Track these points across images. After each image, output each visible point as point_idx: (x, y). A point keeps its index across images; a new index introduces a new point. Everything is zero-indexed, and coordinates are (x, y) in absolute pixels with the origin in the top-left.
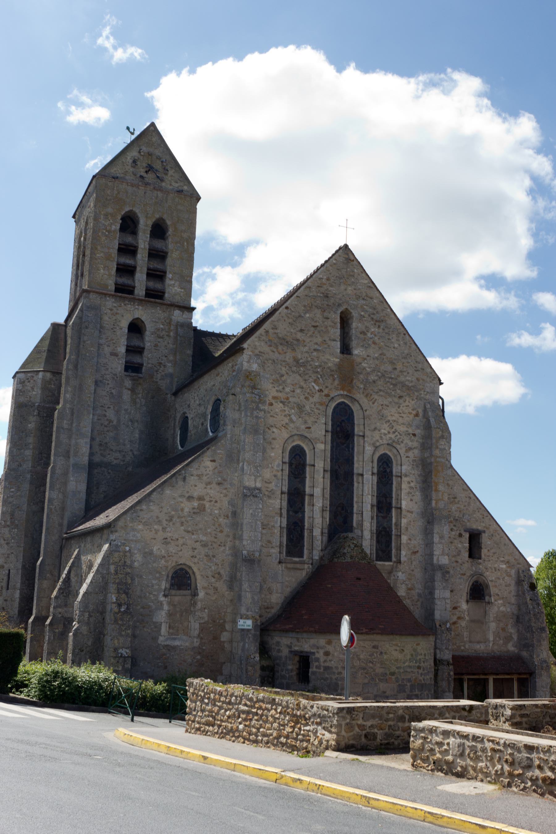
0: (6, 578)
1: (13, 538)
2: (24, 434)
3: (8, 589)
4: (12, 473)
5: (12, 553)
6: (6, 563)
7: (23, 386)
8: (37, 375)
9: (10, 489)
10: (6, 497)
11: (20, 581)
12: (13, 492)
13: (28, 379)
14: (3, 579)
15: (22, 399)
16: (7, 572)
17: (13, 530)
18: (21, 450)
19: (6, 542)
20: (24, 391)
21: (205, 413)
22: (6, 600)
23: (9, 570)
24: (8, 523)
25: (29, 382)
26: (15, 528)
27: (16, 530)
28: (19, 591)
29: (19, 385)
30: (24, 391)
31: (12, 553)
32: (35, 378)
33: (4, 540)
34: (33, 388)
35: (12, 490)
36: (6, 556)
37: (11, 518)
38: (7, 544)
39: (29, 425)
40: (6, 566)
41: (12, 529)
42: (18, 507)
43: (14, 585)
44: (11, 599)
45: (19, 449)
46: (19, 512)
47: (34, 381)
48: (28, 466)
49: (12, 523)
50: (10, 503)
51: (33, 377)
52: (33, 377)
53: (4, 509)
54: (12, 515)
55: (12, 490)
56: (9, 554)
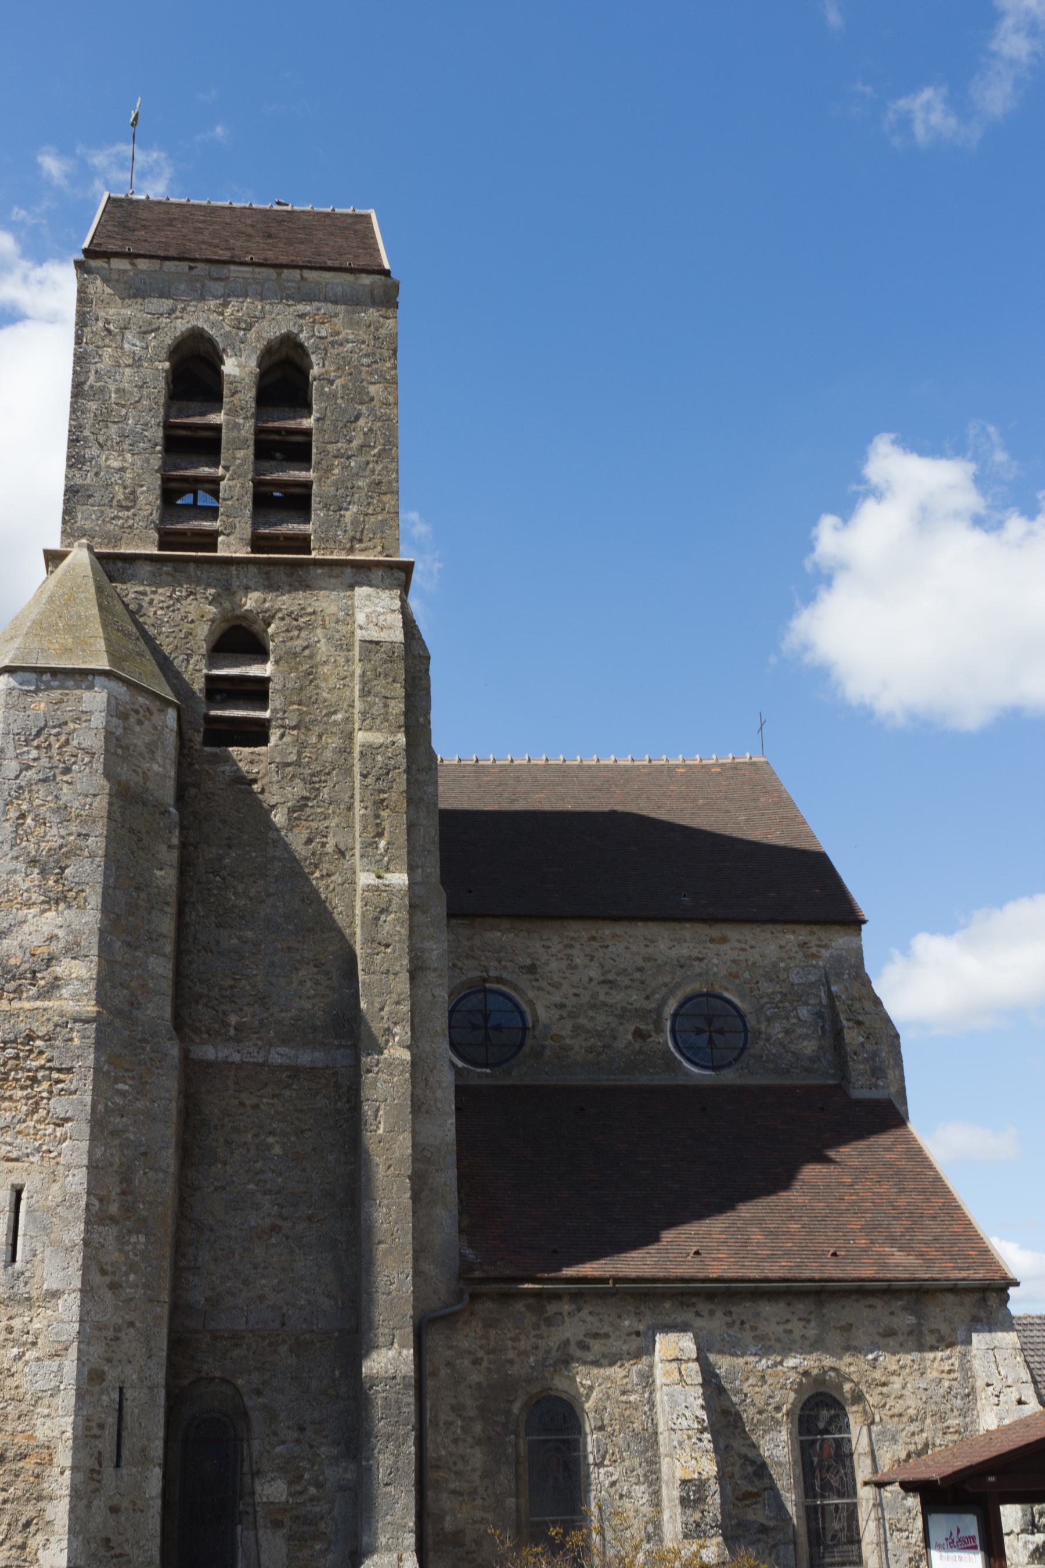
0: (112, 1420)
1: (132, 1268)
2: (143, 895)
3: (118, 1465)
4: (117, 1023)
5: (131, 1324)
6: (109, 1360)
7: (125, 729)
8: (161, 711)
9: (116, 1080)
10: (100, 1107)
11: (161, 1433)
12: (123, 1094)
13: (137, 712)
14: (101, 1426)
15: (124, 772)
16: (116, 1396)
17: (133, 1239)
18: (136, 948)
19: (108, 1279)
20: (127, 748)
21: (659, 1010)
22: (114, 1510)
23: (121, 1389)
24: (114, 1209)
25: (140, 723)
26: (138, 1232)
27: (142, 1239)
28: (158, 1472)
29: (115, 721)
30: (127, 748)
31: (131, 1324)
32: (156, 718)
33: (103, 1272)
34: (151, 749)
35: (121, 1086)
36: (110, 1334)
37: (123, 1193)
38: (114, 1287)
39: (158, 873)
40: (111, 1374)
41: (130, 1232)
42: (145, 1154)
43: (143, 1450)
44: (134, 1503)
45: (129, 945)
46: (151, 1174)
47: (155, 728)
48: (159, 1009)
49: (127, 1210)
50: (114, 1133)
51: (151, 713)
52: (151, 713)
53: (99, 1152)
54: (126, 1178)
55: (121, 1086)
56: (118, 1329)
